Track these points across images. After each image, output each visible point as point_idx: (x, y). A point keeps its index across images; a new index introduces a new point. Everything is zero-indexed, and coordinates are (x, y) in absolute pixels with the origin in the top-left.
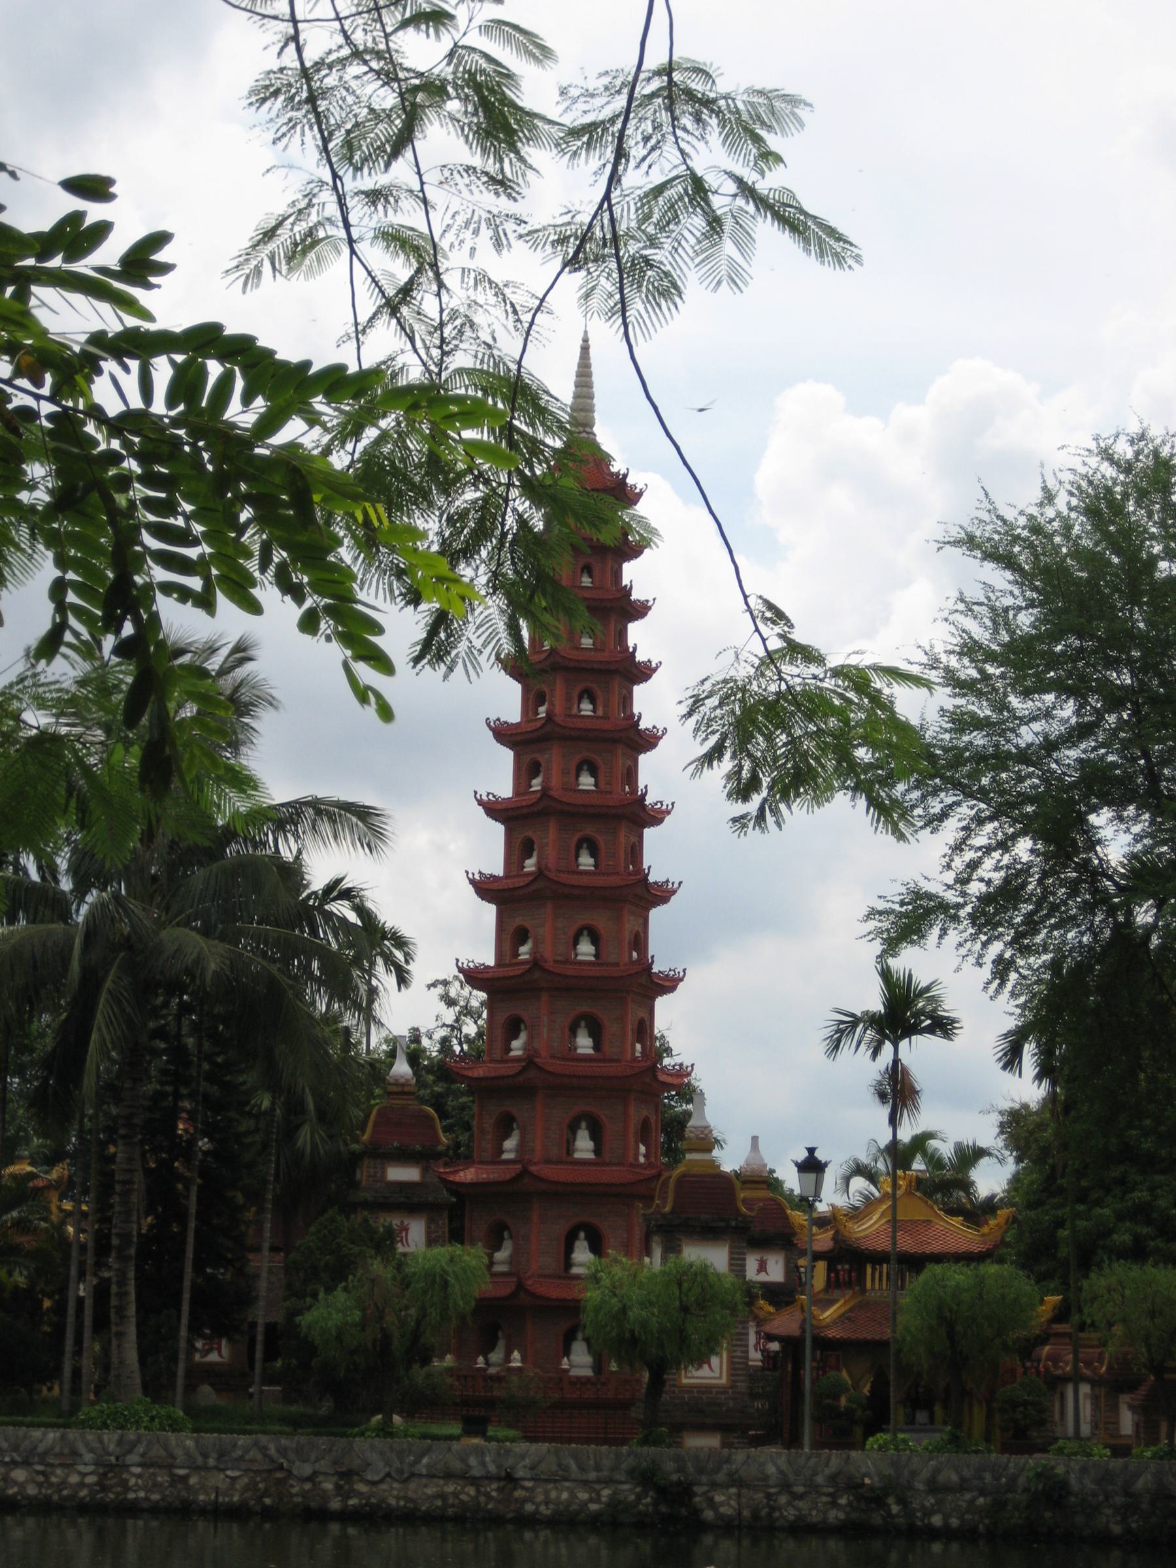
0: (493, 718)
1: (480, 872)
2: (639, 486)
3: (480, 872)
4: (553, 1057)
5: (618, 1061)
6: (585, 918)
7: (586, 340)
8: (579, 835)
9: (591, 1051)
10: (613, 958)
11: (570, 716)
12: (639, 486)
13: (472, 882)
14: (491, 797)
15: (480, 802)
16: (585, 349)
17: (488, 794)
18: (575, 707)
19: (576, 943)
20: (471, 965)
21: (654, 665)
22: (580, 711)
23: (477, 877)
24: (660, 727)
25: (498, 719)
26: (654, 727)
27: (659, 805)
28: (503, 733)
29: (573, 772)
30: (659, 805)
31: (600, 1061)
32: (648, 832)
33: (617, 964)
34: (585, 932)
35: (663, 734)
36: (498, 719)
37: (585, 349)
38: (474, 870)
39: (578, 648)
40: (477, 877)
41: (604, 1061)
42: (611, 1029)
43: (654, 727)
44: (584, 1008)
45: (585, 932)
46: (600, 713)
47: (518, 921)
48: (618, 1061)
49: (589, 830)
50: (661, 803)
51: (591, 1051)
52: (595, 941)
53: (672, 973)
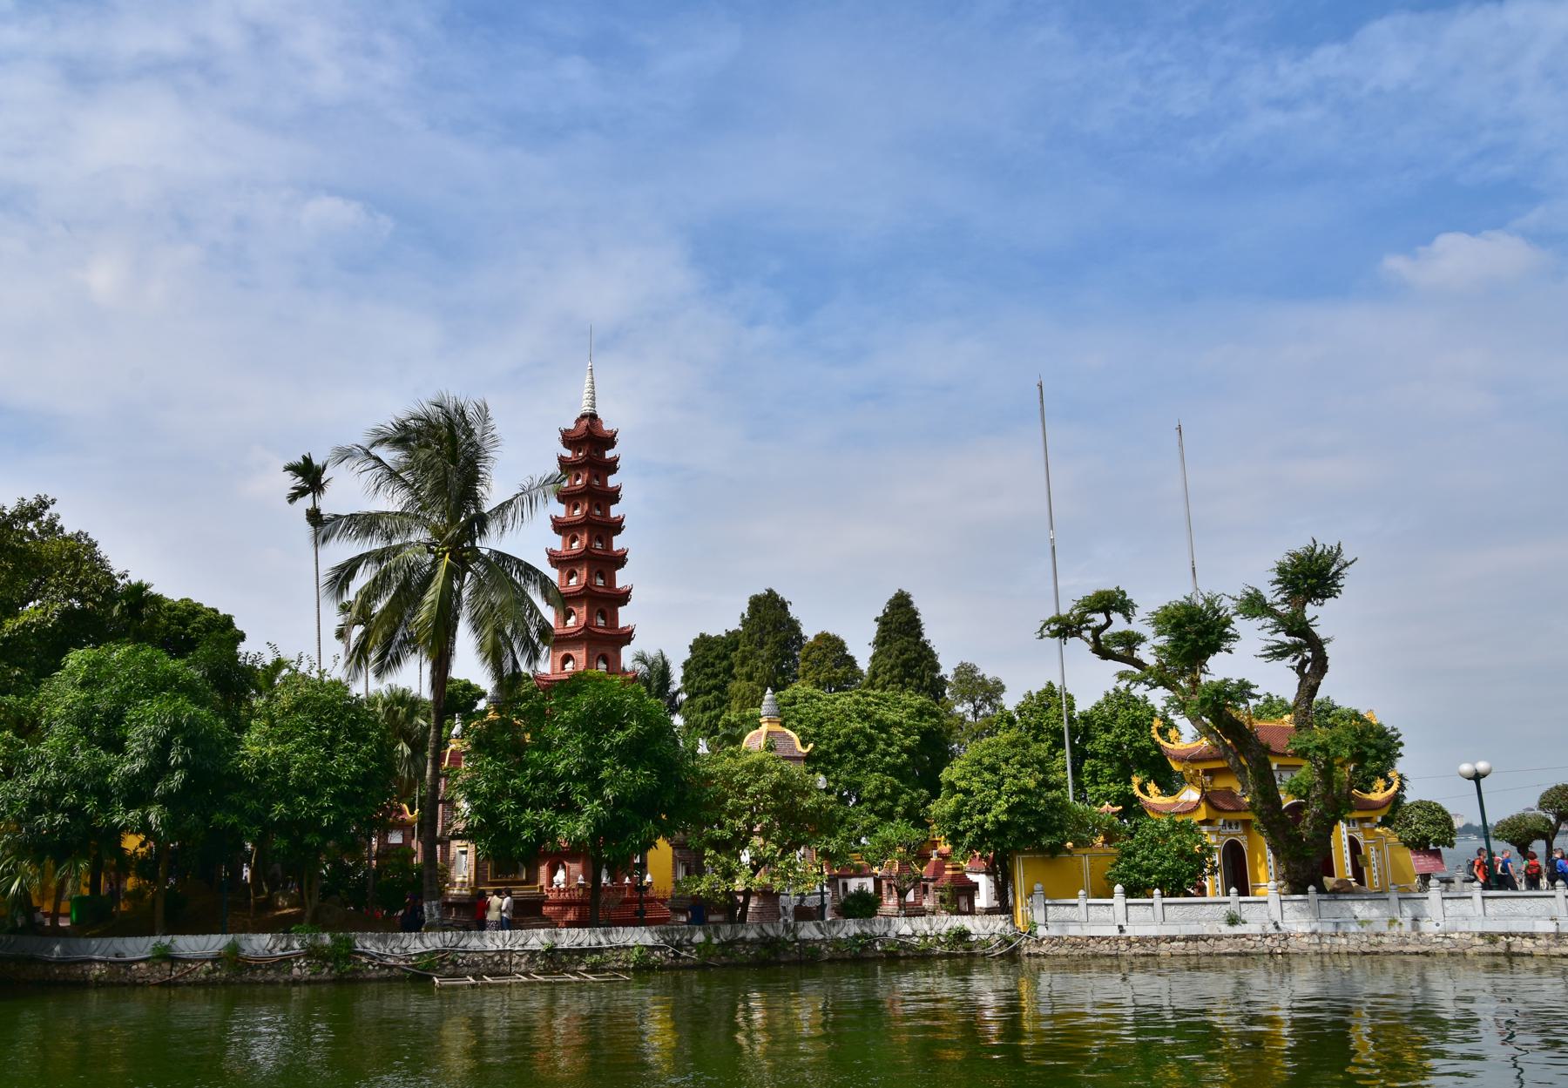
6: (600, 651)
32: (620, 609)
49: (602, 606)
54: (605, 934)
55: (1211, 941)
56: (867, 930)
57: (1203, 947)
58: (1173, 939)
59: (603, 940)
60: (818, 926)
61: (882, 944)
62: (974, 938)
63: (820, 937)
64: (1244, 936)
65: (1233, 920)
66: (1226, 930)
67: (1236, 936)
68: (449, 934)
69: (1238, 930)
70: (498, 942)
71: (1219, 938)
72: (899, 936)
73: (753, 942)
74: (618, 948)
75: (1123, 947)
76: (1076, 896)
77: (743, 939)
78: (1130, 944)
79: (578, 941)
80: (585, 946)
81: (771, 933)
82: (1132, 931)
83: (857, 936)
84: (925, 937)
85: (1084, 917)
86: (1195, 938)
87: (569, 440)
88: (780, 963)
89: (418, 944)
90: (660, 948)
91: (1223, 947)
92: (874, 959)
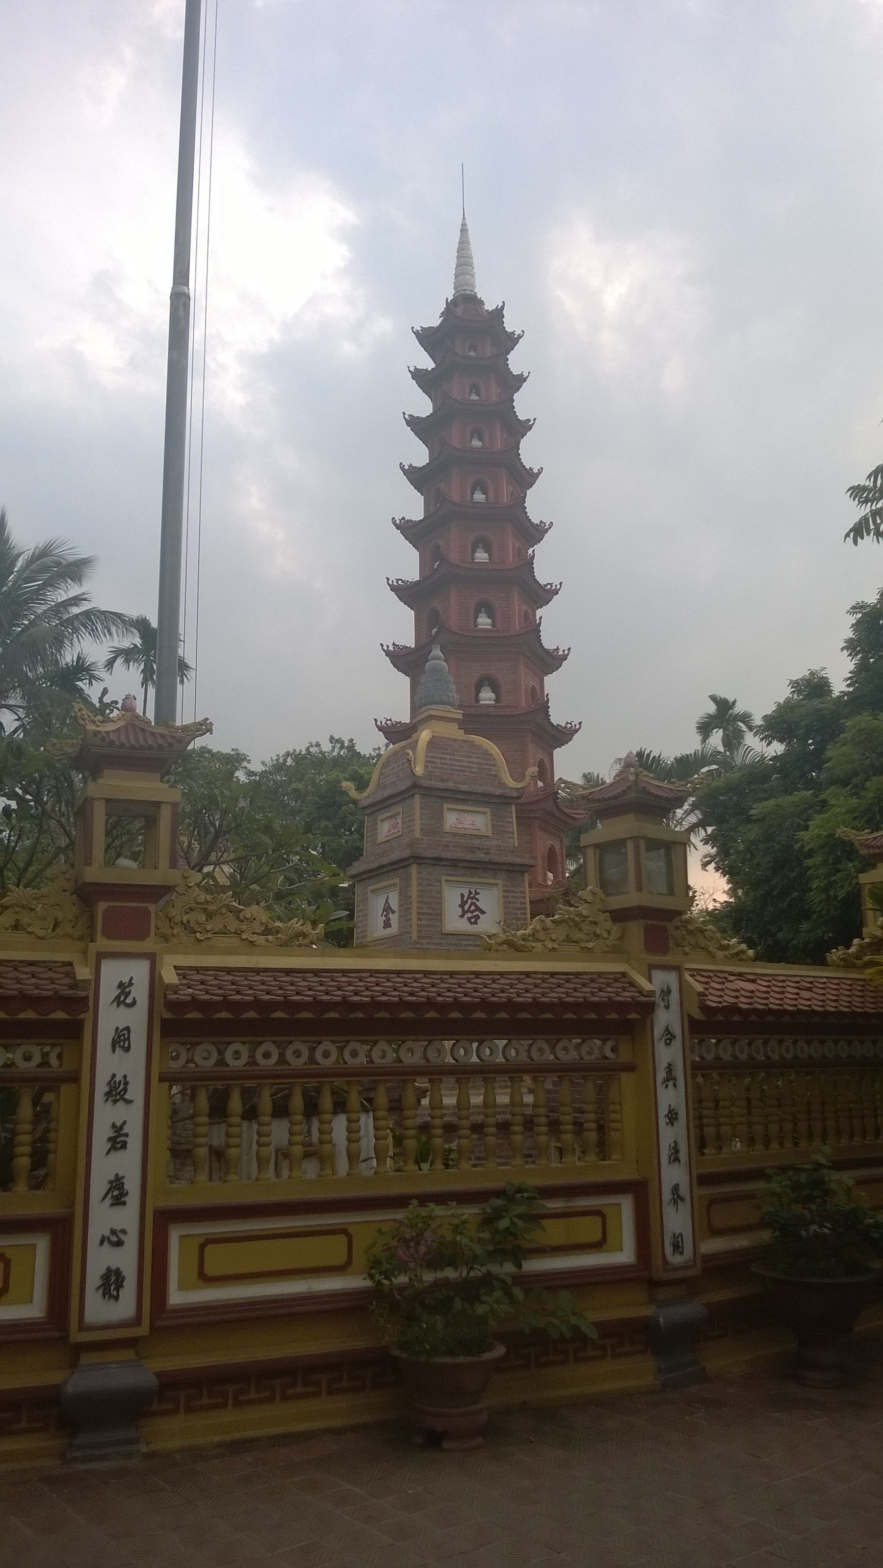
1: (394, 644)
3: (394, 644)
12: (517, 333)
13: (388, 653)
14: (400, 582)
16: (464, 230)
17: (397, 580)
19: (478, 692)
20: (389, 722)
21: (535, 471)
25: (403, 518)
26: (541, 522)
27: (549, 586)
28: (406, 528)
30: (549, 586)
34: (486, 683)
35: (550, 528)
36: (403, 518)
37: (464, 230)
38: (389, 643)
43: (541, 522)
45: (486, 683)
50: (551, 584)
52: (495, 689)
53: (569, 726)
87: (427, 338)
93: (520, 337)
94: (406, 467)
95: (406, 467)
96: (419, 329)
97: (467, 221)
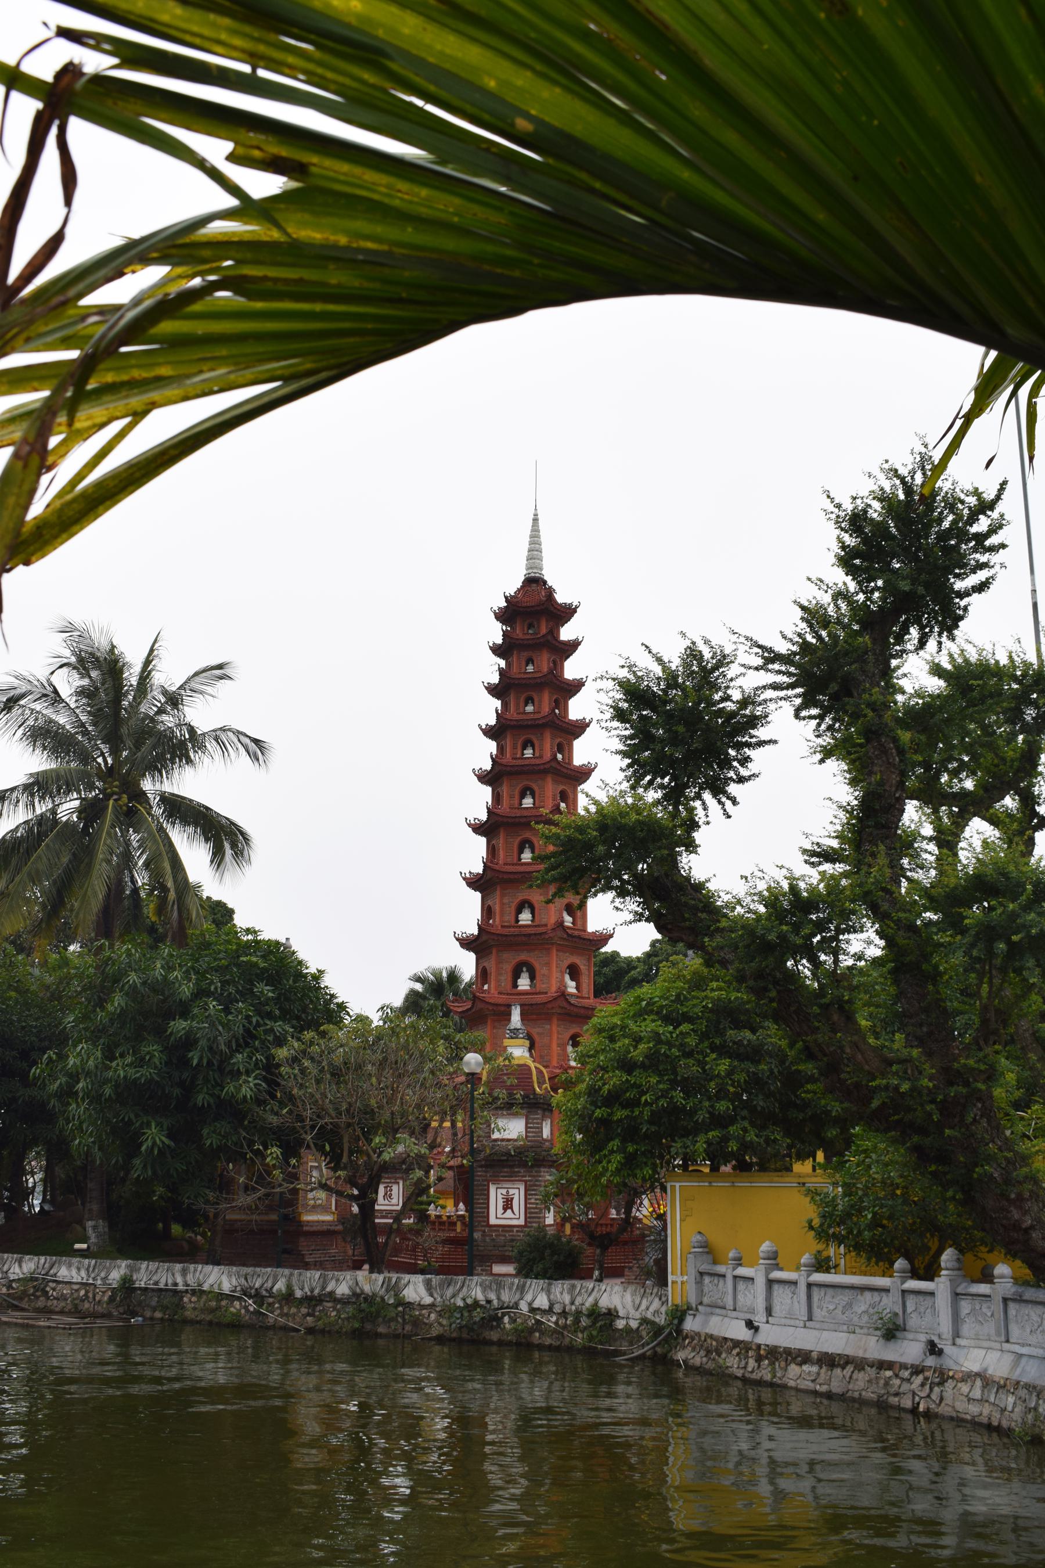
0: (477, 769)
2: (574, 604)
4: (500, 993)
5: (546, 993)
7: (536, 515)
8: (519, 838)
9: (528, 988)
10: (544, 922)
11: (516, 759)
12: (574, 604)
15: (470, 825)
16: (535, 520)
18: (519, 753)
22: (523, 754)
23: (468, 875)
24: (593, 762)
29: (517, 796)
31: (533, 994)
33: (546, 925)
37: (535, 520)
38: (466, 871)
39: (524, 713)
40: (468, 875)
41: (536, 994)
42: (541, 970)
44: (523, 956)
46: (537, 754)
47: (490, 902)
48: (546, 993)
51: (528, 988)
54: (184, 1272)
55: (849, 1369)
56: (492, 1296)
57: (837, 1381)
58: (803, 1357)
59: (179, 1280)
60: (428, 1285)
61: (513, 1321)
62: (620, 1324)
63: (428, 1300)
64: (889, 1365)
65: (892, 1332)
66: (873, 1348)
67: (883, 1365)
68: (42, 1259)
69: (891, 1353)
70: (83, 1273)
71: (859, 1364)
72: (533, 1310)
73: (344, 1301)
74: (194, 1292)
75: (752, 1364)
76: (887, 1272)
77: (332, 1293)
78: (759, 1359)
79: (155, 1278)
80: (162, 1286)
81: (367, 1289)
82: (770, 1335)
83: (476, 1304)
84: (564, 1314)
85: (729, 1303)
86: (829, 1361)
87: (502, 616)
88: (379, 1335)
89: (17, 1270)
90: (239, 1299)
91: (861, 1384)
92: (500, 1343)
93: (577, 607)
94: (484, 727)
95: (484, 727)
96: (496, 609)
97: (539, 512)
